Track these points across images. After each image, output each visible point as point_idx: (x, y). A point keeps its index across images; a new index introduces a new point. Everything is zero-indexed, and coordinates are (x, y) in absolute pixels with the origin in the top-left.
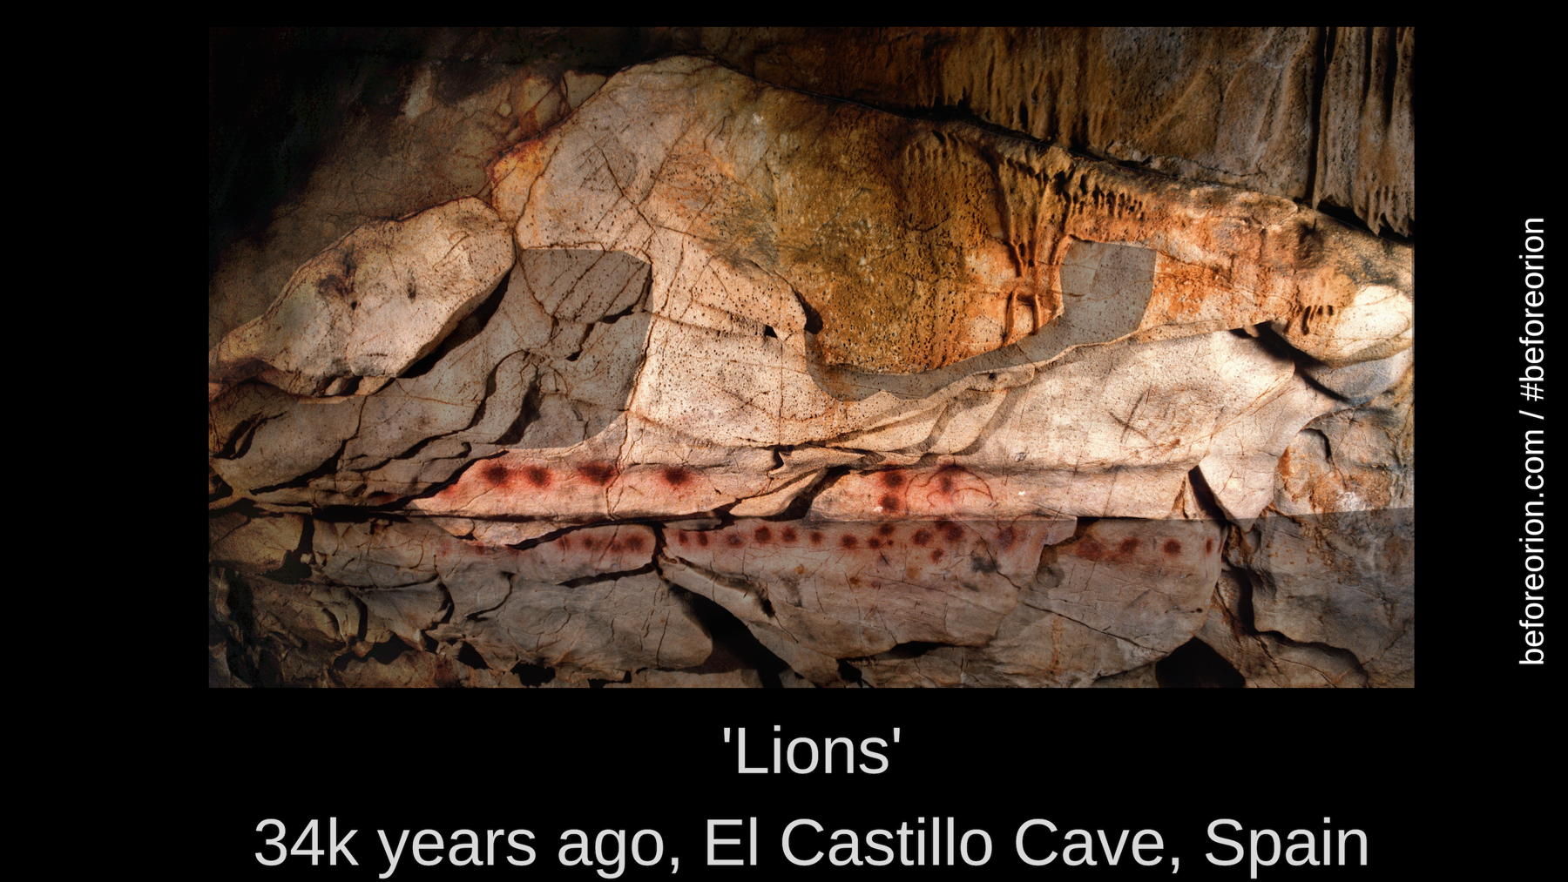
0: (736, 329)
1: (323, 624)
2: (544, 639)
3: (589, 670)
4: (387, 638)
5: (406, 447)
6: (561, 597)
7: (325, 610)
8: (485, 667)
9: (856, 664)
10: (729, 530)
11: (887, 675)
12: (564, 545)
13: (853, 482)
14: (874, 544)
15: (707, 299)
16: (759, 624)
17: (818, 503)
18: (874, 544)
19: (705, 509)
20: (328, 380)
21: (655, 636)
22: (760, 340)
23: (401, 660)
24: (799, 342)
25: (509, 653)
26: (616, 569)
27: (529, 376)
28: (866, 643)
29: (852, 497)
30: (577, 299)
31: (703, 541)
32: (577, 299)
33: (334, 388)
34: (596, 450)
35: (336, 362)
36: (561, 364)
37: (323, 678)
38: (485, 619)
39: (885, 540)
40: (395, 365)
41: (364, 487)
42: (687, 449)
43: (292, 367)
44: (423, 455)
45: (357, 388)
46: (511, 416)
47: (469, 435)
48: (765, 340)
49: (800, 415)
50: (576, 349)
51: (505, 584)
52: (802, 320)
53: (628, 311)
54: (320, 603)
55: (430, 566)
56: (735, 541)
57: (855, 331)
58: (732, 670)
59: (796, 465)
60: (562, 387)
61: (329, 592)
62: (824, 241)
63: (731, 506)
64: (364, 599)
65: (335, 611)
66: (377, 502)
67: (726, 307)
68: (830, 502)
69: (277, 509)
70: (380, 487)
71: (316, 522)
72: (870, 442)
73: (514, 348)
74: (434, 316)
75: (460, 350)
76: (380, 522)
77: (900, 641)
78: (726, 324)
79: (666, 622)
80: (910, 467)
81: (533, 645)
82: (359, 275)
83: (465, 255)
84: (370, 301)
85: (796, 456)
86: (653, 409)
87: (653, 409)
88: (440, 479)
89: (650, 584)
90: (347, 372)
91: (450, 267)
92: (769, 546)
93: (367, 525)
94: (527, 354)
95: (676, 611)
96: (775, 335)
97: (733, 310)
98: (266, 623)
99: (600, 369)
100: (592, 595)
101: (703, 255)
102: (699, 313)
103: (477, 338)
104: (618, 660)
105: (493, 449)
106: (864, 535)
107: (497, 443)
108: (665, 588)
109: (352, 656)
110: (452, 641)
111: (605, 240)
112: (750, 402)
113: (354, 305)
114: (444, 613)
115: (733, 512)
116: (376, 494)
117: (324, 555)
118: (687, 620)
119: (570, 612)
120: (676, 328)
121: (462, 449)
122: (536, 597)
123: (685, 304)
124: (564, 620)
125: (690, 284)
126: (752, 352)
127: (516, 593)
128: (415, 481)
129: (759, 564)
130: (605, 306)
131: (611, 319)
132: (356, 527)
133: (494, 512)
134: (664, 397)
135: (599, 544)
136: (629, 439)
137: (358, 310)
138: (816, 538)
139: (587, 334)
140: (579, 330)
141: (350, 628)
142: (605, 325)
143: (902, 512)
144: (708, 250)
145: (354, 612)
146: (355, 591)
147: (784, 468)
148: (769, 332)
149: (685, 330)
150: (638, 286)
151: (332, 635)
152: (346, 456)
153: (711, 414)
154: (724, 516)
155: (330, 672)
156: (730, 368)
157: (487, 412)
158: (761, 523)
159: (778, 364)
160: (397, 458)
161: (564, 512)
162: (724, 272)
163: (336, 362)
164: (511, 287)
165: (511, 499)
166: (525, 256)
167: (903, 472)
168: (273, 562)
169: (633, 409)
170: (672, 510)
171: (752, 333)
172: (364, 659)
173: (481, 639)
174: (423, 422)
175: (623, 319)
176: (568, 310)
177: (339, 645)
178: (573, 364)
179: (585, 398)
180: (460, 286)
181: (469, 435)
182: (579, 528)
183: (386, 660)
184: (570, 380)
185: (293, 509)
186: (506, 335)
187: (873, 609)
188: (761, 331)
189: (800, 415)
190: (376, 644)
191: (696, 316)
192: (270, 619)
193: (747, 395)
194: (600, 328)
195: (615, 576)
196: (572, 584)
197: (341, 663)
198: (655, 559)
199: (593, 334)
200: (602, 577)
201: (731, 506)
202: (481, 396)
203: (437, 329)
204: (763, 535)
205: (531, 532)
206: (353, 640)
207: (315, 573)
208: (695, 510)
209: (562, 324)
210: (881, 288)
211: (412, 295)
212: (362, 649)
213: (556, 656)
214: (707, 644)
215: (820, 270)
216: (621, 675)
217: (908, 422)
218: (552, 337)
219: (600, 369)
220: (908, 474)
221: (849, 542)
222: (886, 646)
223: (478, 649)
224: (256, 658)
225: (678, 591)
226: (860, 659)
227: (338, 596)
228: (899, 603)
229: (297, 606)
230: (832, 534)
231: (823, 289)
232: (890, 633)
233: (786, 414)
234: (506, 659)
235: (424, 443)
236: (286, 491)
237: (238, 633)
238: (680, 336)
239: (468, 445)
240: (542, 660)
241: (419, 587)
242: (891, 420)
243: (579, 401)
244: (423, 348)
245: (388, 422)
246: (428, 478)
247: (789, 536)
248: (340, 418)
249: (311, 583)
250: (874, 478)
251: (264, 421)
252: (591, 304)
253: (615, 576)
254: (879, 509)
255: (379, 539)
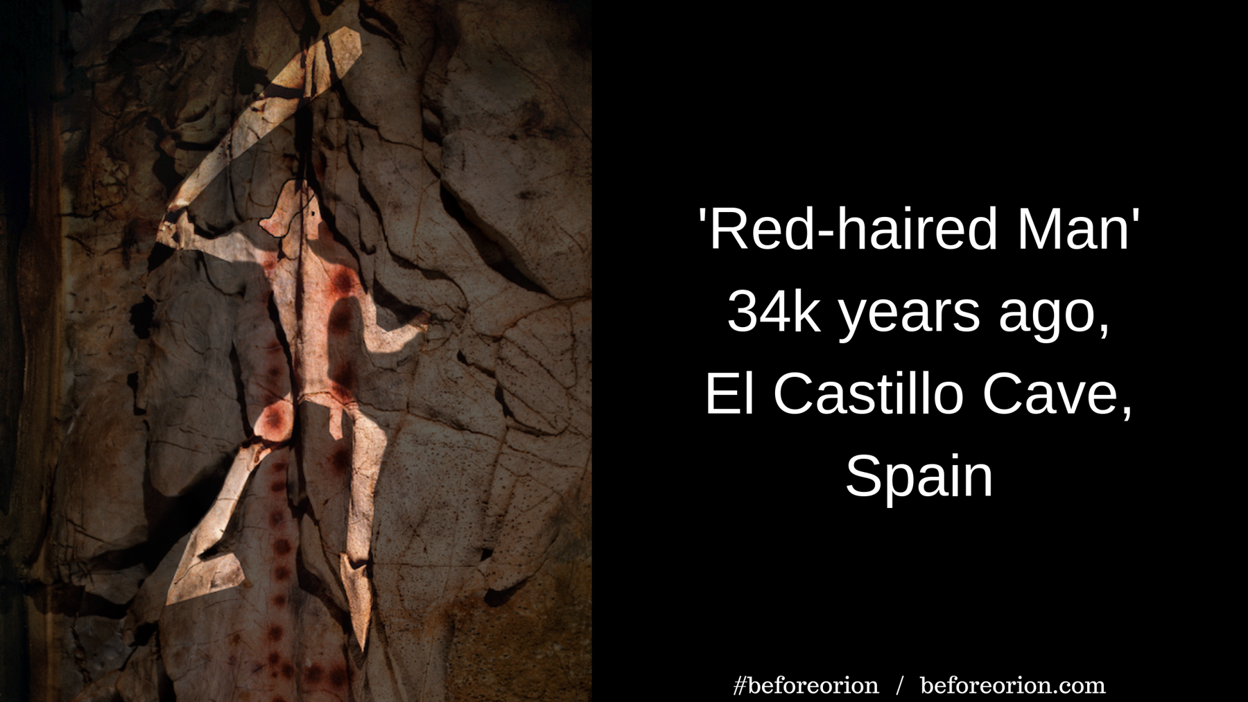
0: (489, 520)
1: (193, 107)
2: (178, 328)
3: (147, 373)
4: (180, 170)
5: (371, 190)
6: (220, 345)
7: (207, 109)
8: (150, 269)
9: (153, 641)
10: (288, 513)
11: (142, 672)
12: (273, 348)
13: (335, 638)
14: (274, 658)
15: (520, 491)
16: (194, 545)
17: (314, 602)
18: (274, 658)
19: (309, 489)
20: (438, 111)
21: (181, 438)
22: (479, 544)
23: (157, 184)
24: (477, 585)
25: (164, 293)
26: (248, 400)
27: (442, 313)
28: (174, 650)
29: (321, 636)
30: (520, 361)
31: (276, 488)
32: (520, 361)
33: (430, 117)
34: (368, 380)
35: (457, 120)
36: (454, 345)
37: (139, 106)
38: (198, 268)
39: (278, 669)
40: (453, 178)
41: (331, 148)
42: (369, 473)
43: (451, 75)
44: (363, 207)
45: (430, 140)
46: (402, 295)
47: (383, 253)
48: (478, 549)
49: (403, 585)
50: (469, 360)
51: (233, 289)
52: (498, 586)
53: (507, 412)
54: (214, 103)
55: (252, 213)
56: (276, 519)
57: (487, 639)
58: (148, 516)
59: (353, 582)
60: (431, 345)
61: (226, 112)
62: (578, 608)
63: (312, 515)
64: (218, 149)
65: (207, 119)
66: (315, 161)
67: (511, 510)
68: (316, 614)
69: (309, 61)
70: (331, 163)
71: (295, 102)
72: (377, 655)
73: (470, 297)
74: (505, 220)
75: (468, 244)
76: (296, 163)
77: (177, 685)
78: (494, 510)
79: (195, 450)
80: (351, 695)
81: (172, 317)
82: (543, 143)
83: (564, 249)
84: (518, 153)
85: (363, 583)
86: (409, 437)
87: (409, 437)
88: (339, 224)
89: (234, 432)
90: (446, 131)
91: (552, 233)
92: (271, 553)
93: (292, 151)
94: (465, 310)
95: (206, 460)
96: (483, 559)
97: (509, 517)
98: (195, 49)
99: (450, 383)
100: (223, 376)
101: (564, 487)
102: (506, 483)
103: (480, 261)
104: (157, 402)
105: (369, 277)
106: (284, 648)
107: (376, 281)
108: (230, 449)
109: (161, 136)
110: (176, 238)
111: (579, 389)
112: (416, 534)
113: (513, 137)
114: (205, 227)
115: (306, 517)
116: (323, 160)
117: (263, 109)
118: (197, 470)
119: (205, 353)
120: (491, 461)
121: (369, 245)
122: (222, 318)
123: (515, 469)
124: (197, 348)
125: (534, 474)
126: (466, 536)
127: (224, 300)
128: (336, 198)
129: (254, 543)
130: (513, 389)
131: (499, 395)
132: (291, 139)
133: (306, 279)
134: (421, 449)
135: (273, 383)
136: (379, 413)
137: (508, 142)
138: (279, 601)
139: (484, 371)
140: (488, 363)
141: (189, 133)
142: (493, 389)
143: (306, 687)
144: (569, 492)
145: (205, 138)
146: (226, 139)
147: (350, 570)
148: (486, 553)
149: (488, 469)
150: (533, 421)
151: (182, 116)
152: (362, 129)
153: (404, 495)
154: (302, 509)
155: (145, 113)
156: (450, 514)
157: (406, 271)
158: (295, 544)
159: (454, 562)
160: (360, 181)
161: (307, 349)
162: (547, 508)
163: (457, 120)
164: (531, 295)
165: (320, 296)
166: (563, 309)
167: (345, 687)
168: (256, 56)
169: (410, 417)
170: (307, 456)
171: (486, 536)
172: (158, 147)
173: (178, 265)
174: (397, 207)
175: (500, 406)
176: (508, 351)
177: (172, 122)
178: (455, 357)
179: (420, 369)
180: (533, 244)
181: (383, 253)
182: (289, 362)
183: (156, 170)
184: (438, 353)
185: (309, 78)
186: (485, 290)
187: (208, 658)
188: (488, 545)
189: (403, 585)
190: (172, 160)
191: (502, 481)
192: (199, 54)
193: (423, 531)
194: (491, 384)
195: (241, 399)
196: (234, 355)
197: (154, 125)
198: (258, 440)
199: (484, 377)
200: (241, 386)
201: (312, 515)
202: (422, 264)
203: (489, 220)
204: (282, 547)
205: (287, 316)
206: (177, 136)
207: (245, 98)
208: (308, 479)
209: (494, 346)
210: (530, 665)
211: (524, 196)
212: (168, 145)
213: (161, 339)
214: (173, 491)
215: (549, 604)
216: (142, 405)
217: (396, 692)
218: (481, 336)
219: (450, 383)
220: (343, 693)
221: (275, 633)
222: (171, 670)
223: (168, 261)
224: (159, 39)
225: (227, 463)
226: (158, 645)
227: (221, 121)
228: (214, 684)
229: (211, 81)
230: (284, 617)
231: (530, 608)
232: (184, 675)
233: (404, 570)
234: (158, 290)
235: (375, 208)
236: (327, 71)
237: (183, 21)
238: (483, 464)
239: (372, 251)
240: (157, 325)
241: (230, 203)
242: (398, 676)
243: (417, 363)
244: (470, 207)
245: (396, 171)
246: (339, 212)
247: (281, 574)
248: (401, 124)
249: (234, 94)
250: (340, 658)
251: (397, 47)
252: (515, 374)
253: (241, 399)
254: (309, 663)
255: (279, 163)
